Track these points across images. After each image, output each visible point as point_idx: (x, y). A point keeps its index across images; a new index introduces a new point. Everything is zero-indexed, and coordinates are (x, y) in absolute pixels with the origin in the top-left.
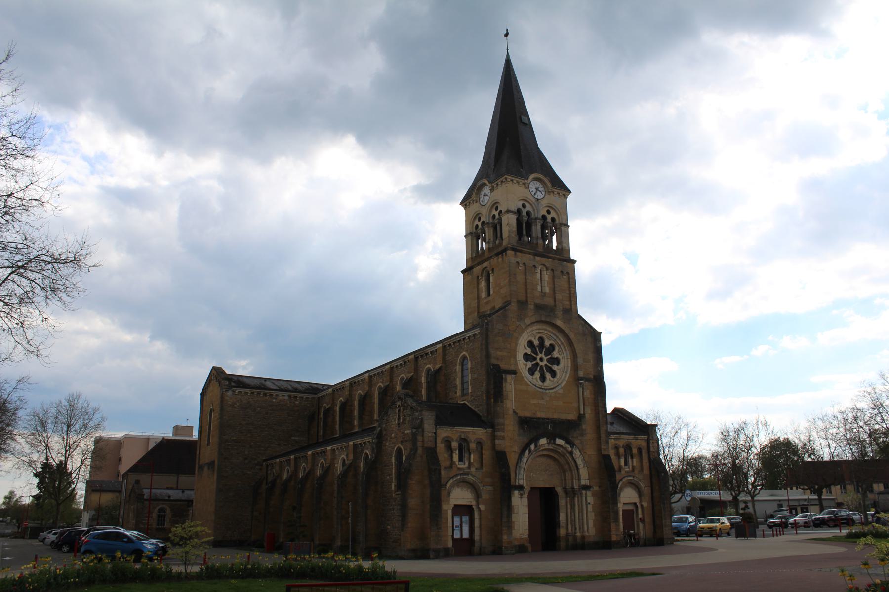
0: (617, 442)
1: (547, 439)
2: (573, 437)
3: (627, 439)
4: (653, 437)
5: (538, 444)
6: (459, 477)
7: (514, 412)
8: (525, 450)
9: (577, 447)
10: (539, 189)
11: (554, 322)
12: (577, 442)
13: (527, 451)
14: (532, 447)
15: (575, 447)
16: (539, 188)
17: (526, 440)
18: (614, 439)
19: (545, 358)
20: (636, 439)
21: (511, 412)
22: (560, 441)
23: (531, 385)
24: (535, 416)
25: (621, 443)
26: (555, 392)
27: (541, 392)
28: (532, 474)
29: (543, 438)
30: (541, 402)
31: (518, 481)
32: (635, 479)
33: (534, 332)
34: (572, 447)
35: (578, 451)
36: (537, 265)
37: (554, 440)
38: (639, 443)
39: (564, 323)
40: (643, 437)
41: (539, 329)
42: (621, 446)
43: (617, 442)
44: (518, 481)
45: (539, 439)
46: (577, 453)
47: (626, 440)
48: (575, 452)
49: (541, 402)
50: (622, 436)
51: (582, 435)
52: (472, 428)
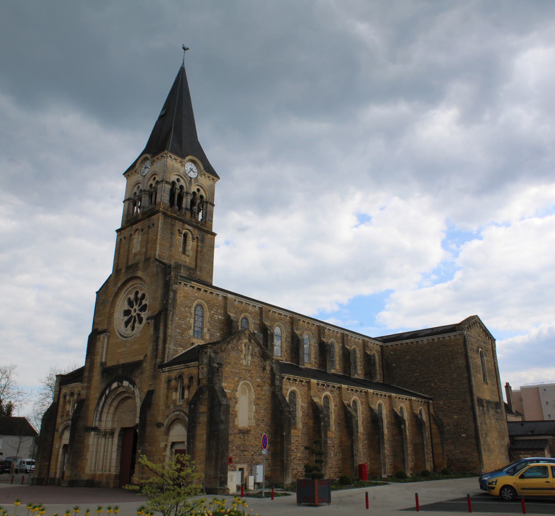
0: (170, 374)
1: (118, 383)
2: (135, 377)
3: (180, 369)
4: (202, 361)
6: (65, 423)
7: (103, 364)
8: (103, 396)
11: (136, 275)
12: (137, 381)
13: (104, 397)
14: (107, 392)
15: (135, 386)
17: (104, 386)
19: (132, 310)
20: (188, 367)
21: (98, 365)
22: (126, 383)
23: (119, 336)
24: (118, 364)
25: (174, 374)
27: (124, 341)
29: (114, 383)
32: (181, 414)
33: (130, 289)
34: (134, 387)
35: (138, 390)
36: (132, 233)
37: (122, 383)
38: (192, 371)
39: (143, 272)
40: (193, 363)
41: (132, 285)
42: (174, 378)
43: (170, 374)
44: (95, 423)
46: (137, 392)
47: (179, 371)
48: (135, 391)
50: (173, 367)
51: (142, 373)
52: (74, 384)
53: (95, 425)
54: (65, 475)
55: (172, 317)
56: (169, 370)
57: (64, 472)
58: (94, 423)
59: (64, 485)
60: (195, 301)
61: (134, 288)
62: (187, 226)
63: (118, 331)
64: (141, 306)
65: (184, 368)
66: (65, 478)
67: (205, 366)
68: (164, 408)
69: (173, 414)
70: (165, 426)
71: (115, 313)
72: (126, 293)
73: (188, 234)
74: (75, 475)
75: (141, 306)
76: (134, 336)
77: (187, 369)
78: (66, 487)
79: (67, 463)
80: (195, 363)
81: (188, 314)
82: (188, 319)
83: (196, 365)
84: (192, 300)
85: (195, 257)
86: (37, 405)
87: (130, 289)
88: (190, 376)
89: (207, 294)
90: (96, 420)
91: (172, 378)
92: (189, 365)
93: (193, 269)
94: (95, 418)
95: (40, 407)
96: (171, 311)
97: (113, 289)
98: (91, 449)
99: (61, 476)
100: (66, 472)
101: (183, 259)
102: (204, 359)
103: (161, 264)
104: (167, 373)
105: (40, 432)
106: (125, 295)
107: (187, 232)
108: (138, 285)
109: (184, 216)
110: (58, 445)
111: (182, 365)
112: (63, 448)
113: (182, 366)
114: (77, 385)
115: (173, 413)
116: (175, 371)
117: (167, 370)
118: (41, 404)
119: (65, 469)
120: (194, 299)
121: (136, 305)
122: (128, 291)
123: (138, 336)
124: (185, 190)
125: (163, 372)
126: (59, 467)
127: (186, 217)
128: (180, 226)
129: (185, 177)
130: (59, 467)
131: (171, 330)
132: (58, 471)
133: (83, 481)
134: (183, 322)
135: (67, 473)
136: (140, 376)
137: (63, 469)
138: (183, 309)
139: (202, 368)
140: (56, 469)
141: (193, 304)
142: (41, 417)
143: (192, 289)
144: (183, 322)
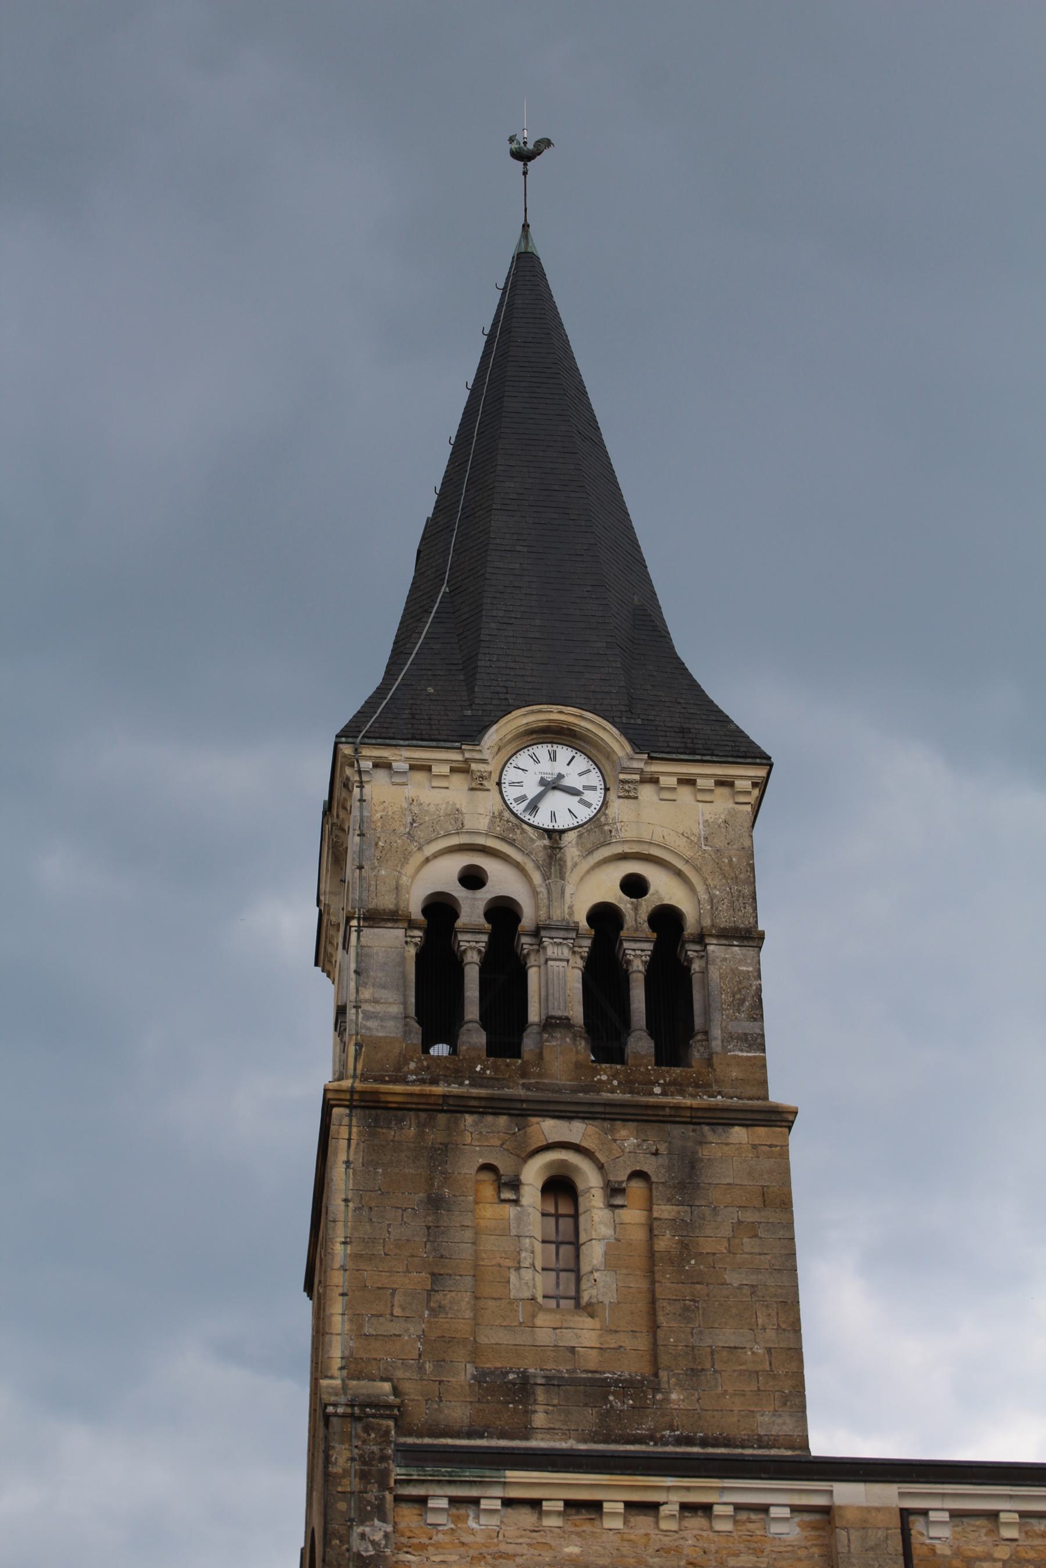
10: (567, 782)
16: (560, 776)
62: (550, 1129)
73: (576, 1169)
85: (642, 1306)
89: (664, 1525)
93: (628, 1386)
107: (563, 1163)
109: (524, 1075)
124: (528, 919)
127: (540, 1075)
128: (497, 1142)
129: (511, 843)
143: (526, 1517)
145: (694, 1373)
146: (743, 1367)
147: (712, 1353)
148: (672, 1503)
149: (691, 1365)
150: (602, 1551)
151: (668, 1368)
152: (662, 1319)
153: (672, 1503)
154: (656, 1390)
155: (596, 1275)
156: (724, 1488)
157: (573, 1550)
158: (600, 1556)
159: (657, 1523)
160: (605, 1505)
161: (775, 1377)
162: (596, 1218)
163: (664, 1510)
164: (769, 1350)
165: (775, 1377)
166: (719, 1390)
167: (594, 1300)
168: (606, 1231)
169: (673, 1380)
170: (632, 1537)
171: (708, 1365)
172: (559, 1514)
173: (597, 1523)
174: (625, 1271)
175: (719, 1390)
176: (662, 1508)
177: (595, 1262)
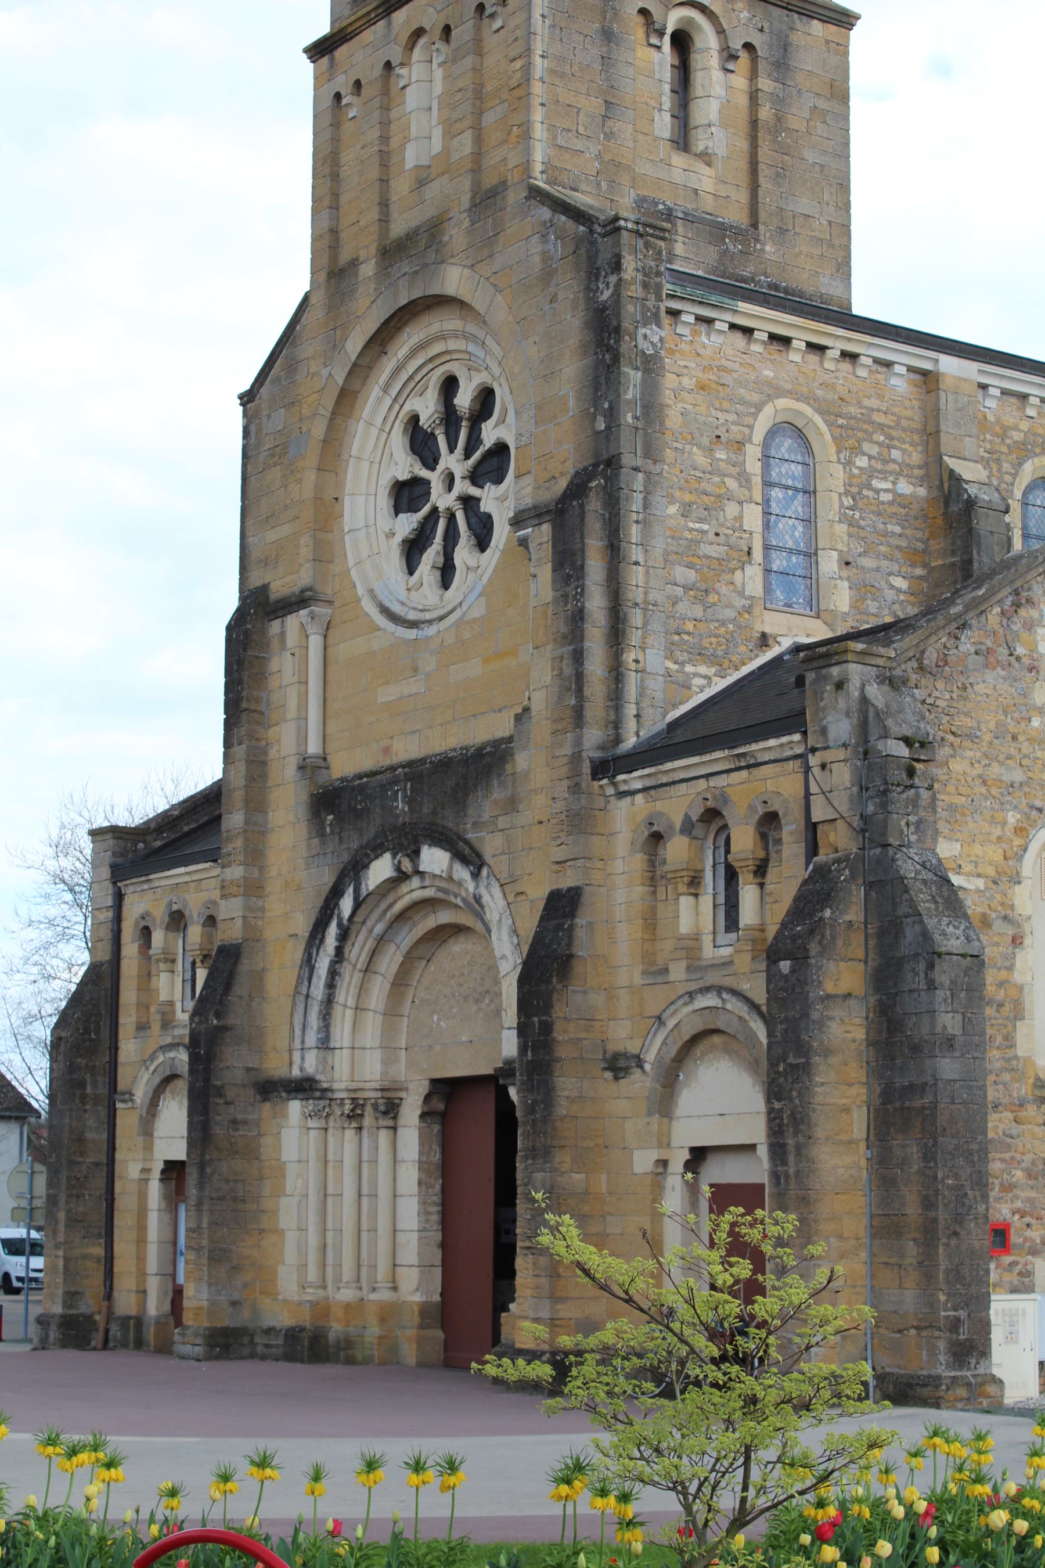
0: (659, 806)
1: (394, 856)
3: (707, 776)
4: (824, 731)
5: (363, 886)
6: (161, 1059)
7: (309, 767)
9: (492, 873)
11: (436, 290)
12: (490, 845)
13: (333, 930)
14: (346, 905)
15: (485, 872)
17: (328, 878)
18: (645, 790)
19: (434, 478)
20: (749, 767)
23: (381, 621)
24: (387, 762)
26: (459, 622)
27: (408, 641)
28: (435, 1018)
30: (412, 686)
31: (303, 1059)
32: (729, 1006)
33: (411, 367)
34: (476, 876)
38: (771, 786)
40: (772, 742)
41: (422, 346)
42: (678, 822)
43: (659, 806)
44: (303, 1059)
45: (366, 866)
46: (494, 901)
47: (702, 784)
48: (486, 899)
49: (412, 686)
50: (669, 766)
51: (512, 805)
52: (182, 870)
53: (301, 1071)
54: (186, 1303)
55: (646, 506)
56: (648, 783)
57: (178, 1293)
58: (297, 1056)
59: (187, 1349)
60: (759, 407)
61: (431, 360)
63: (371, 592)
64: (477, 456)
65: (728, 771)
66: (188, 1318)
67: (841, 754)
68: (638, 979)
69: (690, 1008)
70: (647, 1067)
71: (347, 501)
72: (394, 393)
73: (699, 28)
74: (234, 1304)
75: (477, 456)
76: (457, 614)
77: (744, 773)
78: (199, 1360)
79: (188, 1247)
80: (784, 739)
81: (732, 484)
82: (731, 509)
83: (790, 753)
84: (744, 402)
85: (743, 164)
86: (18, 976)
87: (411, 367)
88: (761, 810)
89: (828, 365)
90: (303, 1042)
91: (671, 827)
92: (751, 754)
93: (738, 234)
94: (298, 1032)
95: (31, 988)
96: (636, 469)
97: (325, 372)
98: (292, 1183)
99: (167, 1307)
100: (189, 1291)
101: (678, 176)
102: (829, 718)
103: (563, 218)
104: (639, 798)
105: (52, 1104)
106: (388, 401)
107: (690, 21)
108: (452, 344)
110: (140, 1166)
111: (718, 754)
112: (161, 1180)
113: (718, 758)
114: (195, 877)
115: (686, 1004)
116: (684, 785)
117: (638, 785)
118: (35, 970)
119: (181, 1279)
120: (755, 397)
121: (452, 449)
122: (404, 377)
123: (477, 612)
125: (621, 795)
126: (152, 1265)
130: (152, 1265)
131: (647, 572)
132: (153, 1285)
133: (269, 1331)
134: (706, 527)
135: (195, 1297)
136: (502, 822)
137: (174, 1276)
138: (700, 459)
139: (823, 766)
140: (142, 1274)
141: (751, 427)
142: (43, 1032)
143: (739, 339)
144: (706, 527)
145: (782, 231)
146: (813, 234)
147: (794, 217)
148: (837, 349)
149: (780, 225)
150: (787, 378)
151: (765, 223)
152: (762, 181)
153: (837, 349)
154: (757, 240)
155: (713, 129)
156: (873, 344)
157: (768, 373)
158: (786, 382)
159: (821, 362)
160: (794, 341)
161: (832, 246)
162: (714, 78)
163: (831, 354)
164: (830, 223)
165: (832, 246)
166: (797, 250)
167: (710, 151)
168: (719, 90)
169: (768, 234)
170: (806, 370)
171: (790, 227)
172: (764, 343)
173: (784, 354)
174: (733, 131)
175: (797, 250)
176: (828, 351)
177: (711, 117)
